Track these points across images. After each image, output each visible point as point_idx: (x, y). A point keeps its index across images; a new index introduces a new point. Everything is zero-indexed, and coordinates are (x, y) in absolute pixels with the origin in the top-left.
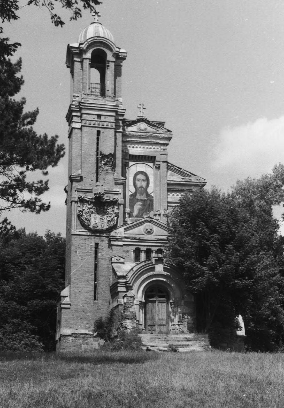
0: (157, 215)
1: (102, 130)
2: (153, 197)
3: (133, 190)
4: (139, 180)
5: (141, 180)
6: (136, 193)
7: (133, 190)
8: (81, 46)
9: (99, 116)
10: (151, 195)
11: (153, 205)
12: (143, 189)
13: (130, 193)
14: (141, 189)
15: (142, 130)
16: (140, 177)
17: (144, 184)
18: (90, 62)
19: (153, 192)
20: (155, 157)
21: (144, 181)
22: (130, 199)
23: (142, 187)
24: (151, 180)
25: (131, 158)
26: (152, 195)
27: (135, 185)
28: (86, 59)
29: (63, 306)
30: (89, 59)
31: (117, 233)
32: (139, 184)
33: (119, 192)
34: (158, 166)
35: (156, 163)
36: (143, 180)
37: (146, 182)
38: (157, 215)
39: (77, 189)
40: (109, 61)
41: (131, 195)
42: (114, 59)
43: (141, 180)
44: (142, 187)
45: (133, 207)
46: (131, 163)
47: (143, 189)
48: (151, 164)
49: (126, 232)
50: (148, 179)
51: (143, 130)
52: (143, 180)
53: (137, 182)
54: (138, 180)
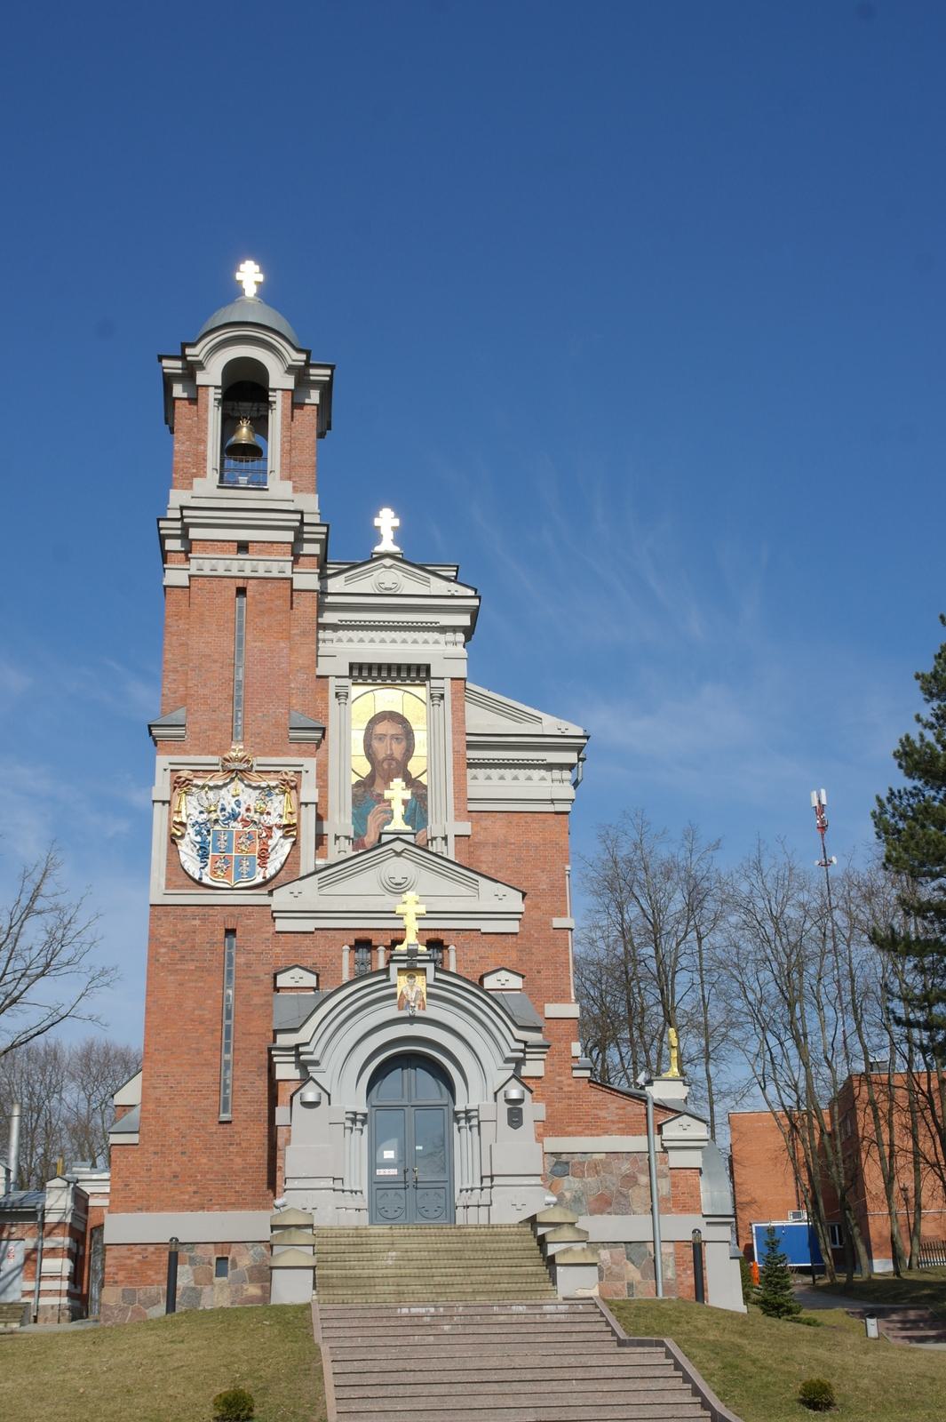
0: (439, 840)
1: (251, 587)
2: (425, 787)
3: (364, 768)
4: (381, 737)
5: (388, 738)
6: (371, 778)
7: (364, 768)
8: (188, 351)
9: (243, 547)
10: (420, 782)
11: (426, 811)
12: (394, 763)
13: (355, 779)
14: (390, 765)
15: (386, 589)
16: (381, 728)
17: (398, 750)
18: (220, 396)
19: (426, 771)
20: (428, 667)
21: (397, 739)
22: (355, 796)
23: (391, 758)
24: (421, 738)
25: (355, 673)
26: (424, 779)
27: (370, 754)
28: (208, 386)
29: (114, 1139)
30: (216, 387)
31: (296, 894)
32: (381, 750)
33: (302, 765)
34: (437, 693)
35: (434, 683)
36: (395, 737)
37: (404, 743)
38: (439, 840)
39: (170, 764)
40: (274, 390)
41: (358, 784)
42: (289, 382)
43: (388, 738)
44: (391, 758)
45: (366, 820)
46: (356, 691)
47: (394, 763)
48: (422, 692)
49: (326, 891)
50: (408, 734)
51: (391, 589)
52: (395, 737)
53: (375, 744)
54: (380, 739)
